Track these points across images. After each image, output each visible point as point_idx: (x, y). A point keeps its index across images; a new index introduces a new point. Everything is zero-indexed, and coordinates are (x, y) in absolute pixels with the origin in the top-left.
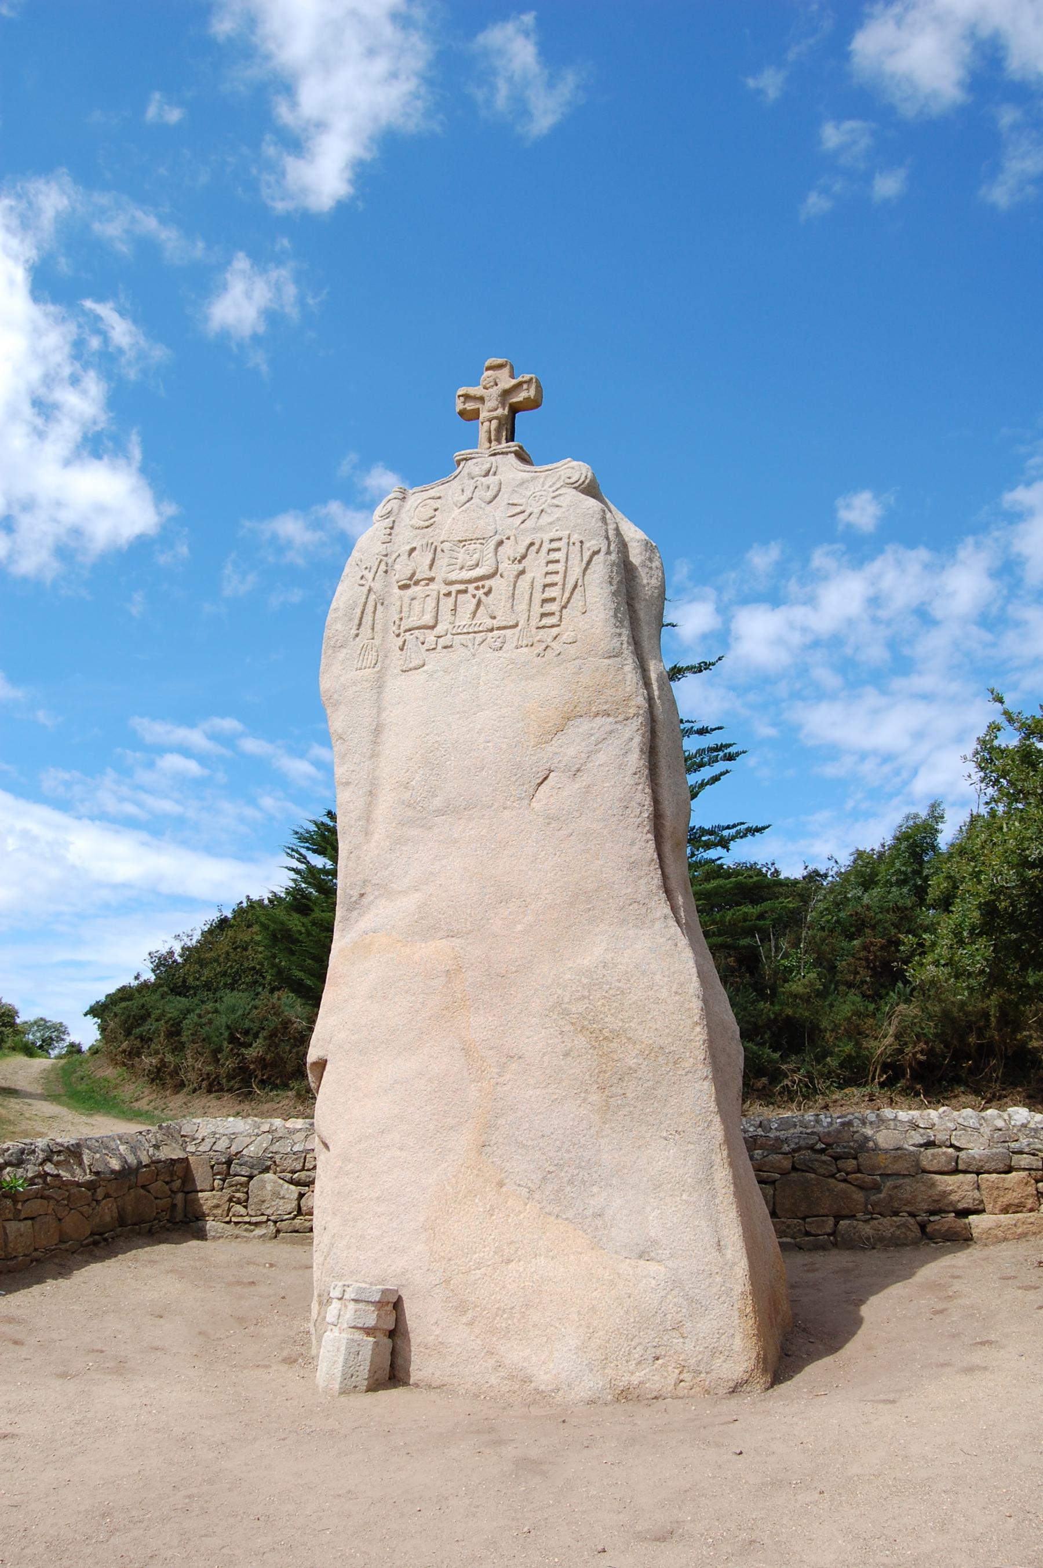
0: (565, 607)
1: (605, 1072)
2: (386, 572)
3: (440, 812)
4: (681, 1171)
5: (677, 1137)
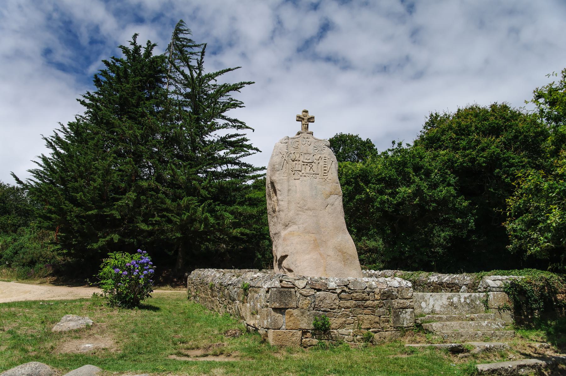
3: (306, 210)
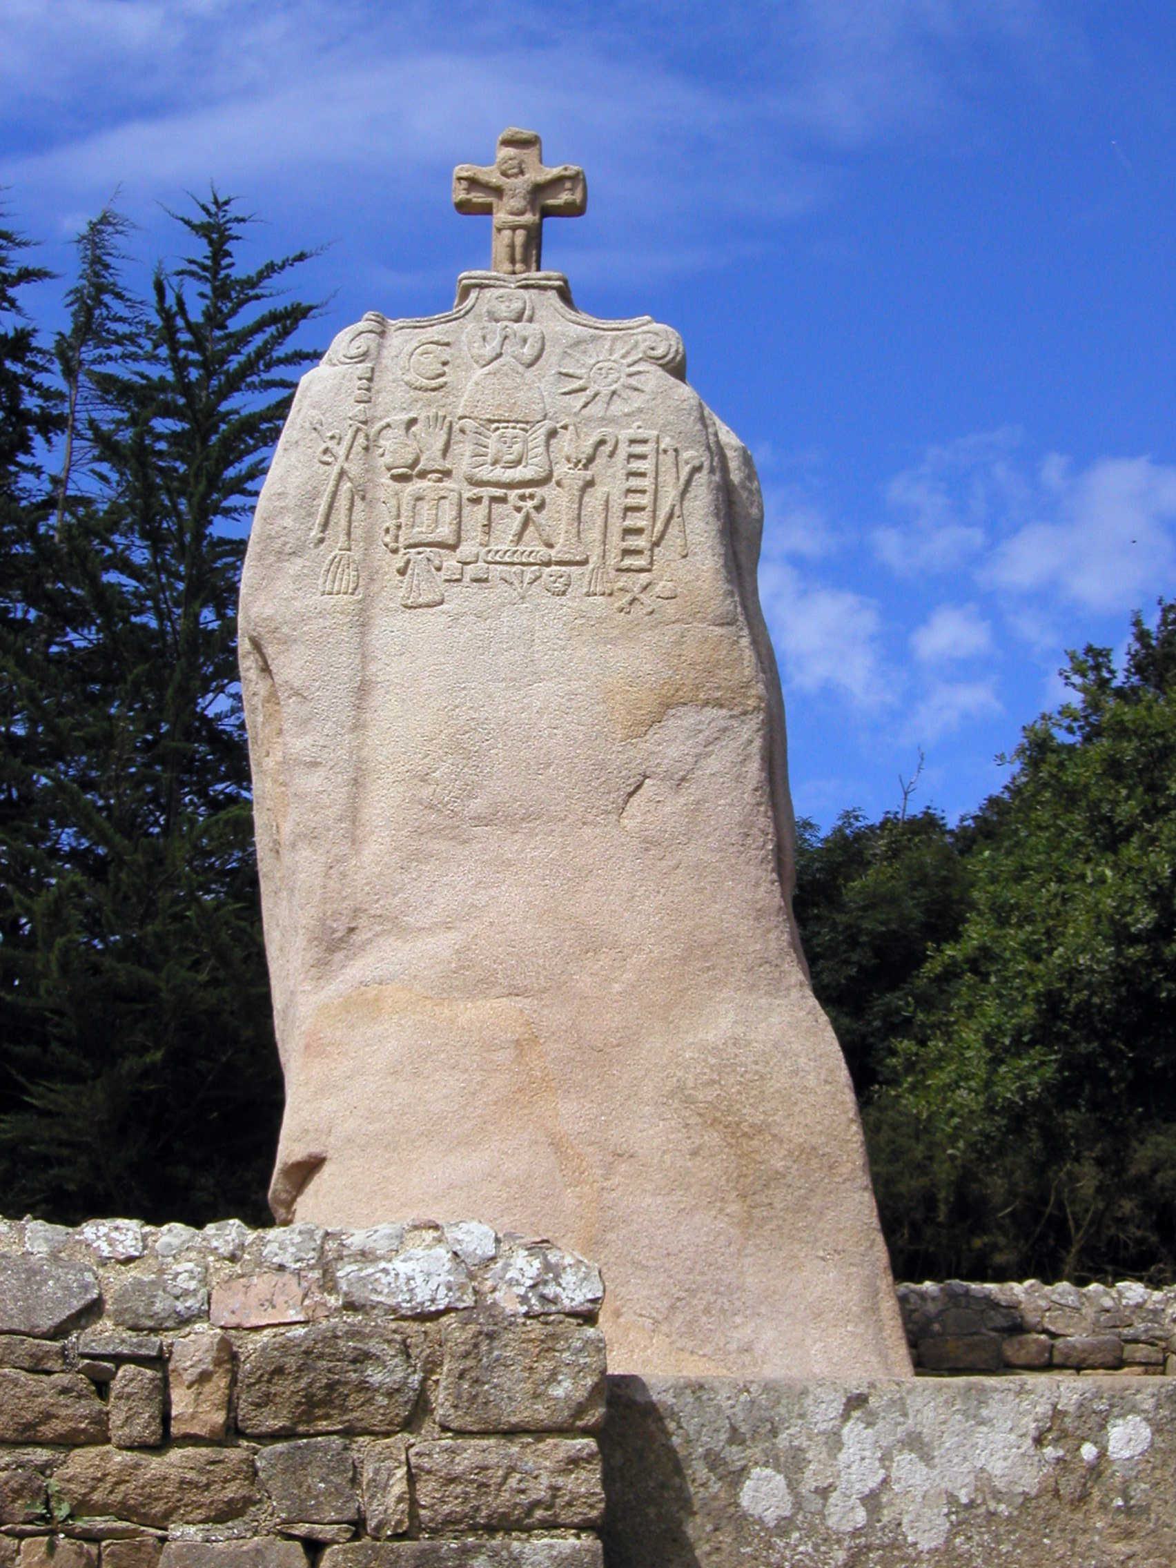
0: (656, 544)
1: (745, 1176)
2: (367, 449)
3: (481, 820)
4: (844, 1298)
5: (837, 1257)
